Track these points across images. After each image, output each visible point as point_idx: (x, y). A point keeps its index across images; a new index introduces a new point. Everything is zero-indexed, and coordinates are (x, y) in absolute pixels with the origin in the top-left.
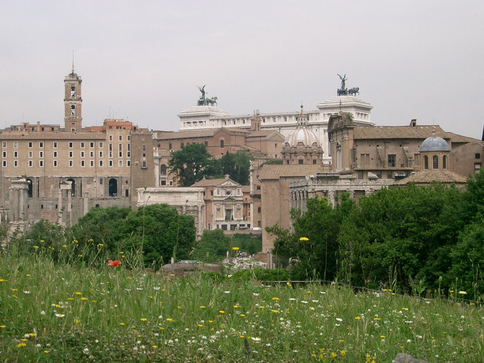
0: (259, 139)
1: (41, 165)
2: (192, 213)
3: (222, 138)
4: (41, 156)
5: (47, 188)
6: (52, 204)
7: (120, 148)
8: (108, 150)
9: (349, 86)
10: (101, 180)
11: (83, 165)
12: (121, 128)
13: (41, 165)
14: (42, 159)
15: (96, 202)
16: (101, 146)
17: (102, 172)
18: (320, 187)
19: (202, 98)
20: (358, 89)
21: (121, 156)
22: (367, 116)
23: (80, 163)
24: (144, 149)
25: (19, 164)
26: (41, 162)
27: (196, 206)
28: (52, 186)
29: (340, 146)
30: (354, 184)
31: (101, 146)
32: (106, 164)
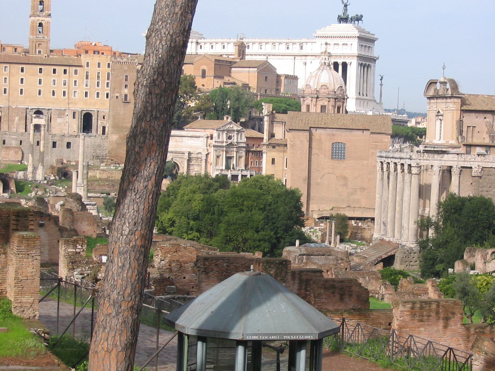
0: (248, 69)
1: (5, 92)
2: (195, 161)
3: (205, 67)
4: (5, 82)
5: (10, 121)
6: (16, 139)
8: (84, 78)
9: (351, 13)
10: (74, 113)
11: (53, 94)
12: (99, 53)
13: (5, 92)
15: (67, 140)
17: (75, 103)
18: (425, 161)
20: (362, 16)
21: (98, 86)
22: (371, 48)
24: (126, 80)
28: (17, 118)
29: (442, 115)
30: (461, 160)
31: (76, 72)
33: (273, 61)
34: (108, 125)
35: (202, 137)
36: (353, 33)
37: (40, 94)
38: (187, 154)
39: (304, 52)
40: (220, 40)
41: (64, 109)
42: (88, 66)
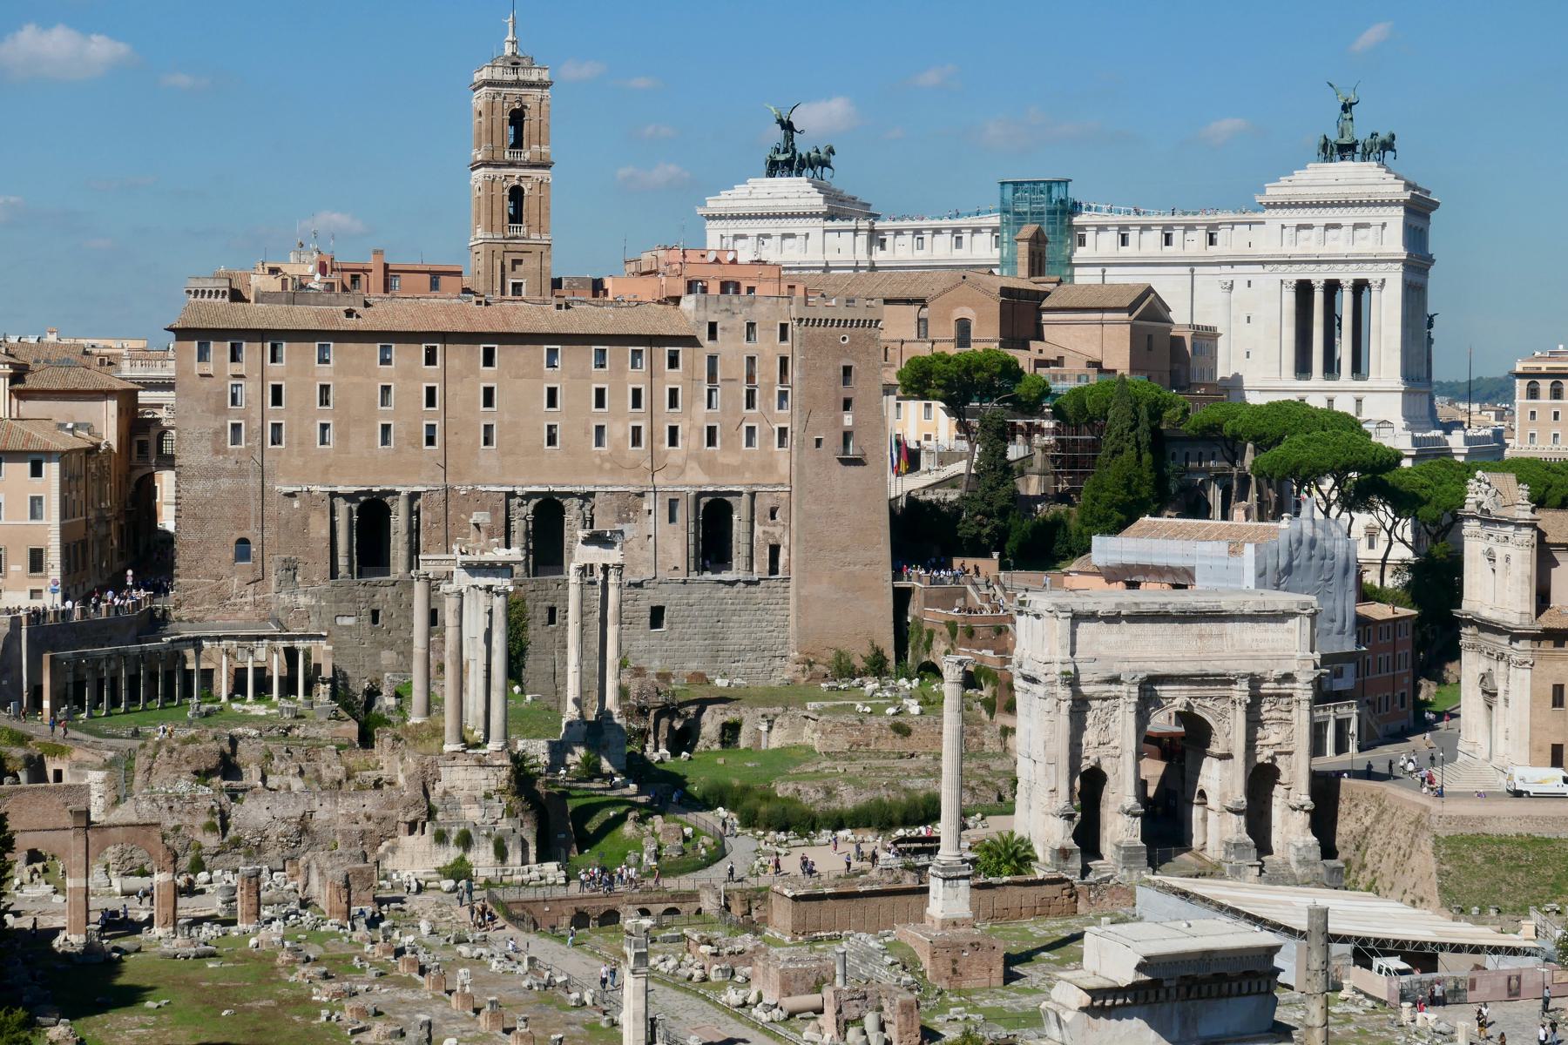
0: (1097, 316)
1: (430, 441)
3: (967, 313)
7: (750, 378)
9: (1360, 132)
10: (673, 504)
11: (599, 443)
12: (737, 292)
13: (430, 441)
14: (435, 416)
16: (673, 362)
19: (786, 151)
20: (1393, 137)
21: (750, 404)
23: (587, 432)
25: (343, 437)
26: (431, 428)
27: (1288, 677)
31: (673, 362)
32: (691, 438)
33: (1170, 288)
34: (786, 539)
35: (1293, 615)
36: (1389, 189)
37: (552, 440)
38: (1245, 685)
39: (1220, 250)
40: (946, 222)
41: (638, 490)
42: (713, 333)
